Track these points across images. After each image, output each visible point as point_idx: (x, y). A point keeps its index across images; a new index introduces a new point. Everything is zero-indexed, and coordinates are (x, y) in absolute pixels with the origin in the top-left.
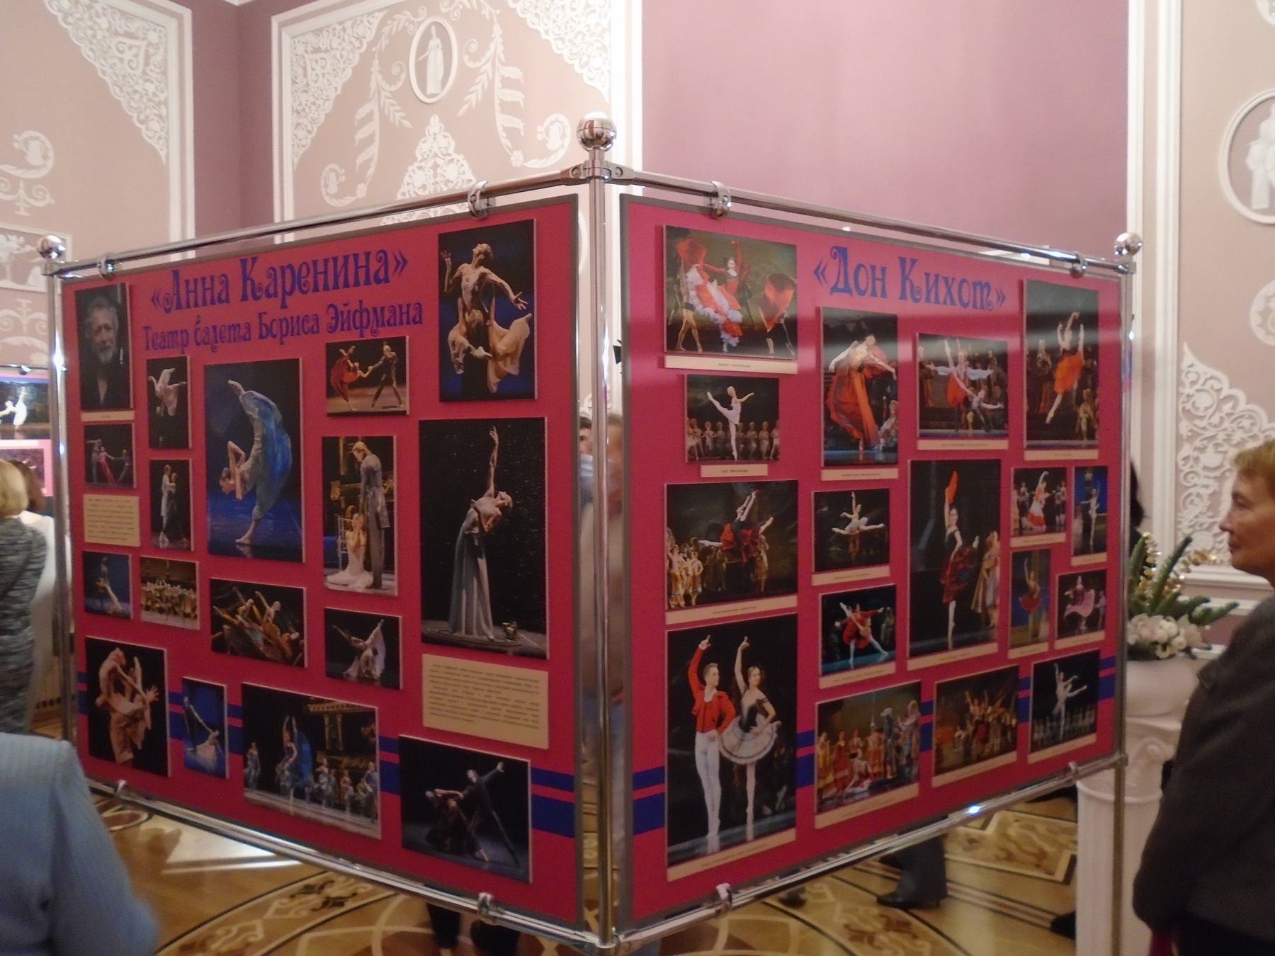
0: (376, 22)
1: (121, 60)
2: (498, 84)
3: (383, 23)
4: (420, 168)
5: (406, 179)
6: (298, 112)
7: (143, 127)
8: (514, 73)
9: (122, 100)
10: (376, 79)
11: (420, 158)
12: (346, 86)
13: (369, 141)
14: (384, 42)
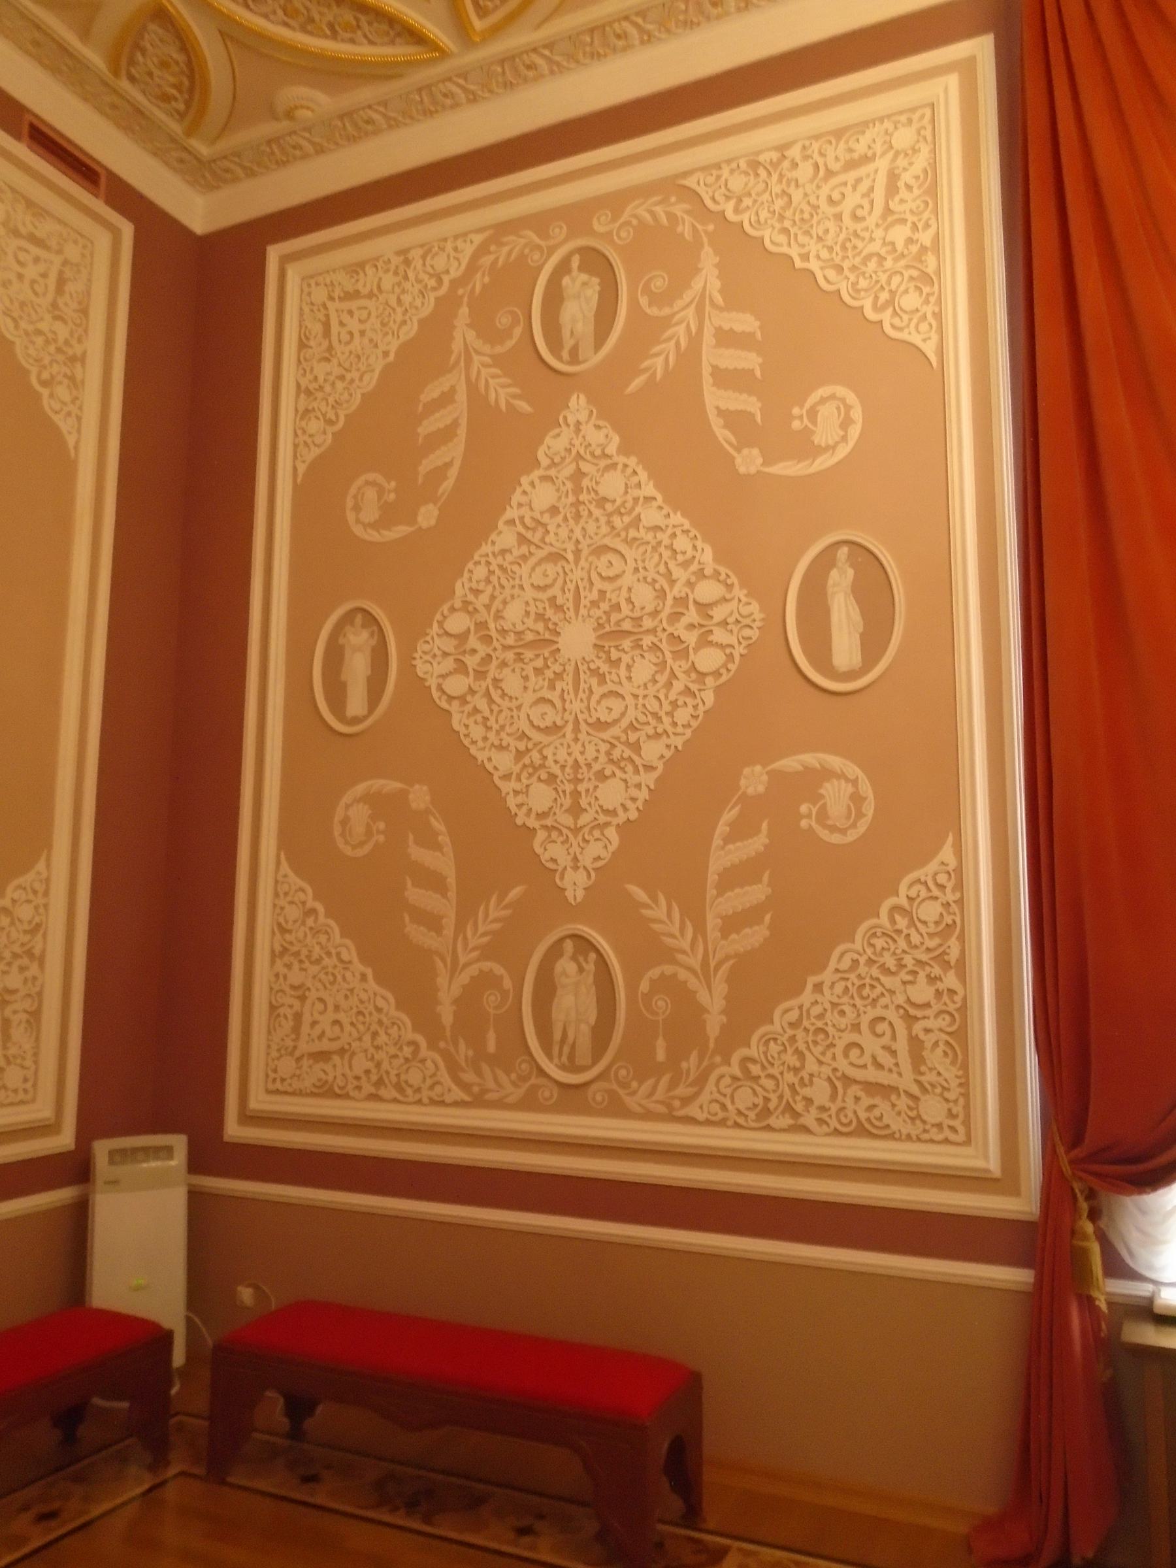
0: (468, 250)
1: (20, 277)
2: (708, 338)
3: (482, 250)
4: (544, 478)
5: (517, 497)
6: (309, 393)
7: (45, 392)
8: (745, 322)
9: (18, 341)
10: (463, 334)
11: (544, 462)
12: (405, 349)
13: (448, 434)
14: (480, 281)
